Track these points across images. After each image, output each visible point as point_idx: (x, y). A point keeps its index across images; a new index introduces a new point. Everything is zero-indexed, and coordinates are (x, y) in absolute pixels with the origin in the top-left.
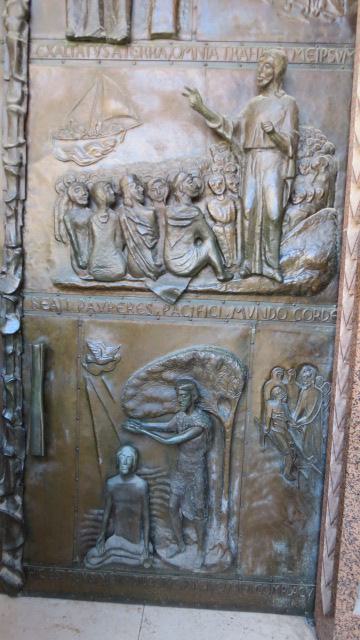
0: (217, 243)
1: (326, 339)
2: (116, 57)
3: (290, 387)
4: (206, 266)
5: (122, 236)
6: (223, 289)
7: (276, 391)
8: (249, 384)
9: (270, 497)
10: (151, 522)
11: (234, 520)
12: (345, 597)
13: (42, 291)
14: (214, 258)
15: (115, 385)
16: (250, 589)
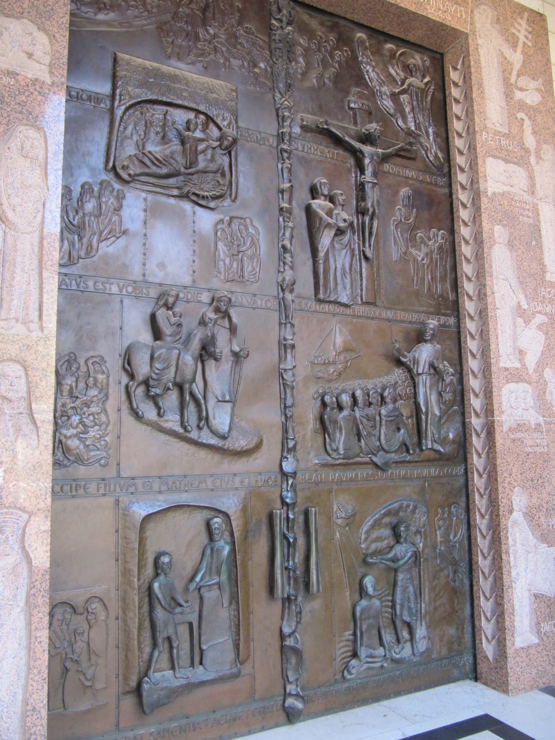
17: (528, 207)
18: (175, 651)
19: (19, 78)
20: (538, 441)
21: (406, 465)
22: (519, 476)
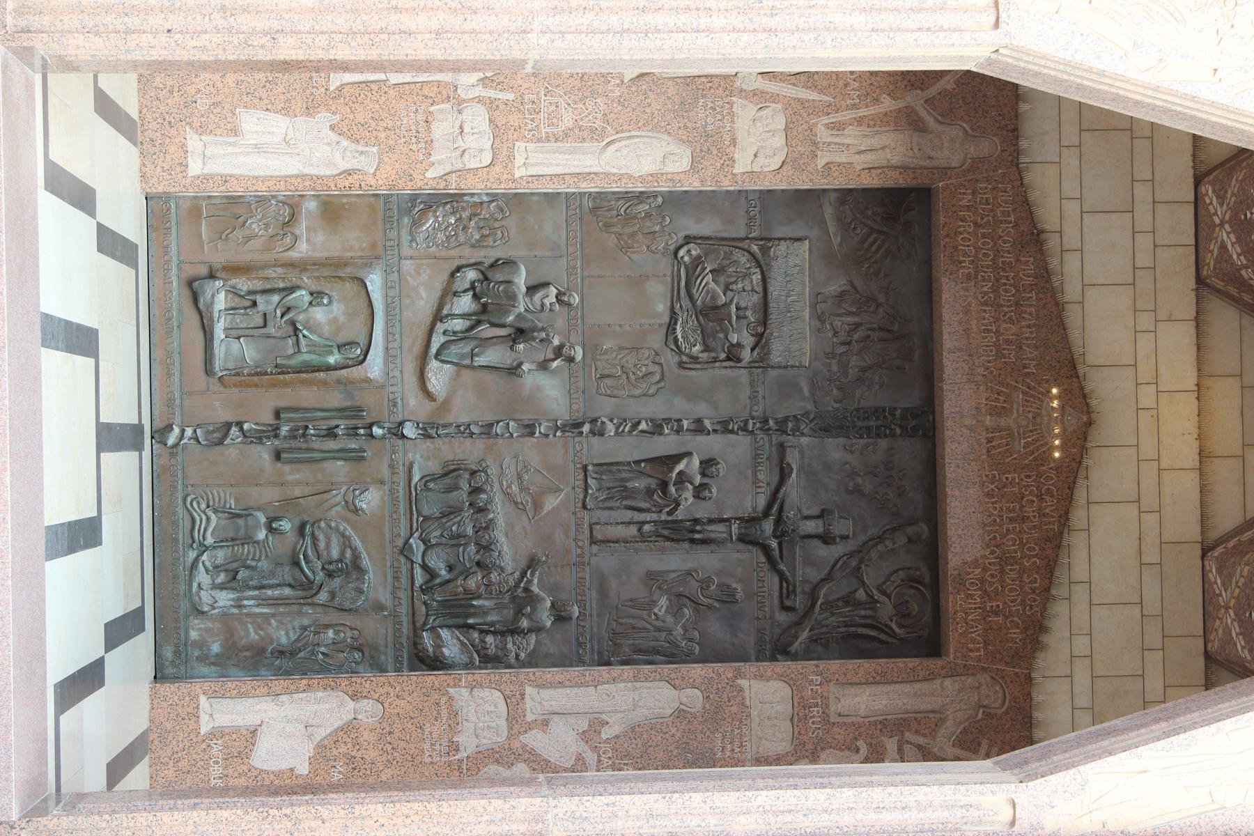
0: (448, 581)
2: (577, 500)
4: (430, 574)
5: (451, 513)
6: (415, 589)
7: (342, 635)
8: (346, 613)
10: (228, 546)
11: (235, 611)
12: (213, 688)
13: (406, 452)
14: (438, 581)
15: (337, 512)
17: (737, 750)
18: (242, 311)
19: (732, 148)
20: (437, 747)
22: (396, 711)
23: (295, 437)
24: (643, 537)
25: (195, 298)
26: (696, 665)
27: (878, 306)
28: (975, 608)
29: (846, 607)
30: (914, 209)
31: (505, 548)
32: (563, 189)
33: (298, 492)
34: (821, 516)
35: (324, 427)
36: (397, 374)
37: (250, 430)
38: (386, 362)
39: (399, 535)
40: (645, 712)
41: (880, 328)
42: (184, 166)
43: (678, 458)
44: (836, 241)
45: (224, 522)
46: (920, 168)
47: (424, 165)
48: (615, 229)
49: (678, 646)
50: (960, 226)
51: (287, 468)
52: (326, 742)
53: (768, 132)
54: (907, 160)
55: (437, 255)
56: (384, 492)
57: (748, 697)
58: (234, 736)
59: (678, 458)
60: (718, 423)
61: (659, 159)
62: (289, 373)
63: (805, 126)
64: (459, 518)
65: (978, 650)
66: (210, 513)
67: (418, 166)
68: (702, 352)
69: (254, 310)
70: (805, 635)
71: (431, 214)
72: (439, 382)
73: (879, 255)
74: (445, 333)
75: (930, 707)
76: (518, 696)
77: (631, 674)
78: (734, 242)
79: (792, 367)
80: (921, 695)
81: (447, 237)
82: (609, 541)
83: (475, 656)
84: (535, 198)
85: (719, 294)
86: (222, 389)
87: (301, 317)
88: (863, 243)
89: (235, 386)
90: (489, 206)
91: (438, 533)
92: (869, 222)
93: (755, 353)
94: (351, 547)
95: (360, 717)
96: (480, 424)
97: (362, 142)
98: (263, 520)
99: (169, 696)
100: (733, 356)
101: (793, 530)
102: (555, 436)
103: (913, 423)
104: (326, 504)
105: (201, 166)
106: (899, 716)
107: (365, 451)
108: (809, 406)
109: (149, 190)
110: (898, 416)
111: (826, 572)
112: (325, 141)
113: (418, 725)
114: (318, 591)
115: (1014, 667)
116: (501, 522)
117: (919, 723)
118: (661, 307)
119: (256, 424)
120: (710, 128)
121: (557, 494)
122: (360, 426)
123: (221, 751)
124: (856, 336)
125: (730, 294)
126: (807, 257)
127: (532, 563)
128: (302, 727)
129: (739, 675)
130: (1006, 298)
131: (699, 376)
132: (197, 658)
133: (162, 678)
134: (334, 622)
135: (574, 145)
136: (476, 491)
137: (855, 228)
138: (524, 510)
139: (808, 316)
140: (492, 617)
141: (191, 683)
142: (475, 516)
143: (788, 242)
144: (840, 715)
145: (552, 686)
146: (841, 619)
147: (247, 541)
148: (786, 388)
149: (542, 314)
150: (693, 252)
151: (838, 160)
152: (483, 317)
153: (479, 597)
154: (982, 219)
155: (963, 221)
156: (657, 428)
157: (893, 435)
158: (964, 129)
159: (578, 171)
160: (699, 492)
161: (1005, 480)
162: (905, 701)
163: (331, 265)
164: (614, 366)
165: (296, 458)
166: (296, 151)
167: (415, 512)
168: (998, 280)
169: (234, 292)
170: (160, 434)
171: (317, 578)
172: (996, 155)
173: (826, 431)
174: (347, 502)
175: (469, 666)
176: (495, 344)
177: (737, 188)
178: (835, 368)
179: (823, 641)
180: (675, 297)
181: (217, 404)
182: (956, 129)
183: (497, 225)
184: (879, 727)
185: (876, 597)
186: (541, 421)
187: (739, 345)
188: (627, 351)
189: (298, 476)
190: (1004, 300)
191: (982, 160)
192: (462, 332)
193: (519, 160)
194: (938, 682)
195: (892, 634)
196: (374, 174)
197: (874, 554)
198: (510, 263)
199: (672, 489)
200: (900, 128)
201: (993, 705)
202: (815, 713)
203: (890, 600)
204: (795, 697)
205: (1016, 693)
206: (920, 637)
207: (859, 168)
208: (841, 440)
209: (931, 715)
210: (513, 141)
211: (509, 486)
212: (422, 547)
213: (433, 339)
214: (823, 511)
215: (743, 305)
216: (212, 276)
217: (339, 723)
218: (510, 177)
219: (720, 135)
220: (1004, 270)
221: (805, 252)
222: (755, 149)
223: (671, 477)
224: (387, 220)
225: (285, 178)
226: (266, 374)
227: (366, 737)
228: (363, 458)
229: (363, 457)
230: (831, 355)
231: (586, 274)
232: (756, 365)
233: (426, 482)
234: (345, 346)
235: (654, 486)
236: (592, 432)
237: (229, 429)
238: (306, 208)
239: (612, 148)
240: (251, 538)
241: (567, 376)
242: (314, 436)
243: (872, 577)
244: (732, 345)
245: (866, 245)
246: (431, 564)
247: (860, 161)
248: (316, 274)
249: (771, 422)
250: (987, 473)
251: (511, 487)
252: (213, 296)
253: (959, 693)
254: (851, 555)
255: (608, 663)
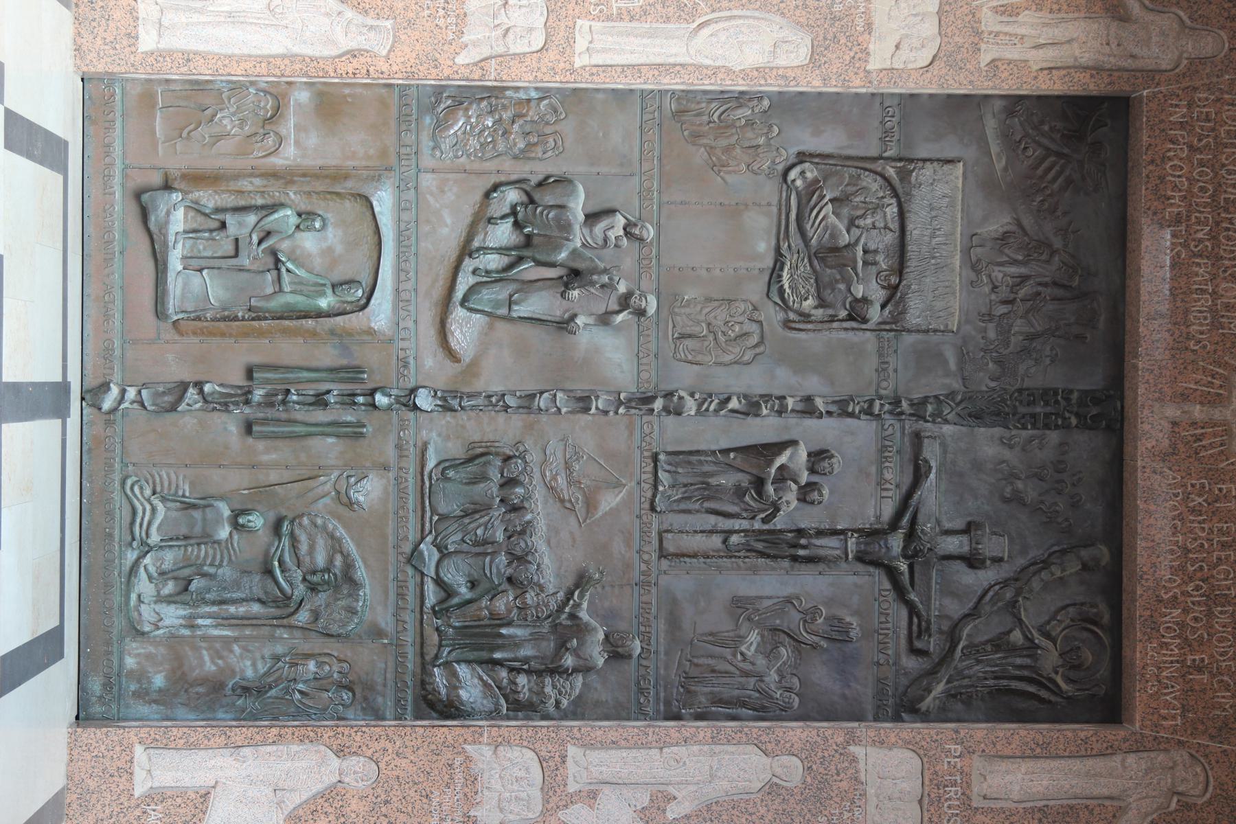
0: (469, 602)
1: (381, 712)
2: (643, 499)
3: (330, 680)
4: (445, 591)
6: (425, 610)
7: (327, 668)
8: (332, 640)
9: (213, 668)
11: (186, 632)
13: (418, 429)
14: (456, 600)
15: (325, 505)
16: (109, 653)
18: (207, 235)
19: (866, 36)
21: (418, 601)
22: (396, 773)
23: (272, 405)
24: (729, 552)
25: (144, 214)
26: (794, 724)
27: (1054, 252)
28: (1172, 662)
29: (996, 652)
30: (1106, 125)
31: (546, 560)
32: (638, 84)
33: (274, 477)
34: (967, 530)
35: (311, 393)
36: (411, 324)
37: (213, 393)
38: (396, 308)
39: (406, 538)
40: (725, 784)
41: (1055, 284)
42: (133, 37)
43: (779, 447)
44: (999, 165)
45: (174, 514)
46: (1119, 70)
47: (453, 47)
48: (705, 141)
49: (772, 697)
50: (1169, 150)
51: (261, 445)
52: (301, 812)
53: (915, 15)
54: (1101, 58)
55: (468, 168)
56: (389, 481)
57: (863, 770)
58: (179, 800)
59: (779, 447)
60: (834, 402)
61: (768, 48)
62: (266, 319)
63: (965, 10)
64: (487, 518)
65: (1174, 717)
66: (156, 502)
67: (446, 48)
68: (816, 307)
69: (223, 234)
70: (939, 688)
71: (461, 113)
72: (465, 338)
73: (1056, 186)
74: (474, 272)
75: (1105, 792)
76: (557, 758)
77: (709, 735)
78: (864, 163)
79: (935, 331)
80: (1095, 775)
81: (481, 145)
82: (683, 555)
83: (503, 701)
84: (600, 96)
85: (841, 231)
86: (177, 337)
87: (285, 245)
88: (1036, 168)
89: (195, 333)
90: (538, 105)
91: (458, 537)
92: (1045, 141)
93: (887, 310)
94: (342, 553)
95: (347, 780)
96: (518, 394)
97: (372, 13)
98: (227, 513)
99: (94, 744)
100: (856, 315)
101: (930, 549)
102: (616, 413)
103: (1094, 411)
104: (310, 494)
105: (156, 38)
106: (1065, 802)
107: (364, 426)
108: (956, 385)
109: (85, 69)
110: (1074, 401)
111: (971, 604)
112: (323, 10)
113: (424, 793)
114: (297, 609)
115: (1221, 743)
116: (541, 526)
117: (1091, 812)
118: (763, 247)
119: (221, 385)
120: (837, 8)
121: (617, 491)
122: (358, 392)
123: (160, 819)
124: (1022, 293)
125: (856, 232)
126: (960, 185)
127: (581, 581)
128: (268, 791)
129: (852, 739)
130: (1228, 248)
131: (813, 341)
132: (134, 693)
133: (87, 719)
134: (317, 651)
135: (654, 25)
136: (509, 483)
137: (1025, 148)
138: (573, 510)
139: (958, 263)
140: (527, 651)
141: (124, 727)
142: (508, 516)
143: (935, 164)
144: (985, 798)
145: (603, 746)
146: (988, 669)
147: (205, 540)
148: (927, 359)
149: (605, 250)
150: (809, 175)
151: (1009, 56)
152: (526, 253)
153: (509, 624)
154: (1200, 140)
155: (1173, 143)
156: (752, 407)
157: (1067, 427)
158: (1180, 18)
159: (658, 60)
160: (806, 493)
161: (1217, 492)
162: (1074, 782)
163: (326, 177)
164: (698, 323)
165: (273, 432)
166: (284, 22)
167: (428, 508)
168: (1217, 224)
169: (196, 208)
170: (92, 395)
171: (296, 593)
172: (1223, 54)
173: (977, 418)
174: (338, 493)
175: (493, 715)
176: (541, 289)
177: (871, 90)
178: (992, 334)
179: (963, 696)
180: (782, 233)
181: (170, 357)
182: (1169, 17)
183: (548, 130)
184: (1038, 815)
185: (1036, 641)
186: (599, 393)
187: (865, 300)
188: (716, 304)
189: (274, 456)
190: (1225, 250)
191: (1202, 61)
192: (498, 272)
193: (581, 44)
194: (1118, 758)
195: (1058, 692)
196: (387, 58)
197: (1036, 584)
198: (563, 181)
199: (770, 489)
200: (1093, 15)
201: (1192, 792)
202: (952, 794)
203: (1055, 645)
204: (926, 771)
205: (1223, 777)
206: (1094, 696)
207: (1035, 68)
208: (998, 431)
209: (1107, 803)
210: (574, 17)
211: (554, 478)
212: (436, 555)
213: (460, 279)
214: (969, 524)
215: (872, 246)
216: (167, 187)
217: (319, 787)
218: (568, 67)
219: (852, 17)
220: (1227, 210)
221: (957, 178)
222: (896, 38)
223: (769, 473)
224: (403, 119)
225: (268, 59)
226: (236, 319)
227: (354, 807)
228: (361, 435)
229: (362, 433)
230: (988, 317)
231: (665, 199)
232: (888, 327)
233: (444, 469)
234: (341, 285)
235: (745, 484)
236: (666, 410)
237: (185, 391)
238: (296, 100)
239: (706, 32)
240: (209, 536)
241: (635, 333)
242: (298, 403)
243: (1031, 615)
244: (856, 300)
245: (1040, 172)
246: (447, 577)
247: (1038, 59)
248: (308, 189)
249: (905, 404)
250: (1194, 482)
251: (556, 480)
252: (168, 213)
253: (1146, 773)
254: (1005, 583)
255: (677, 717)
